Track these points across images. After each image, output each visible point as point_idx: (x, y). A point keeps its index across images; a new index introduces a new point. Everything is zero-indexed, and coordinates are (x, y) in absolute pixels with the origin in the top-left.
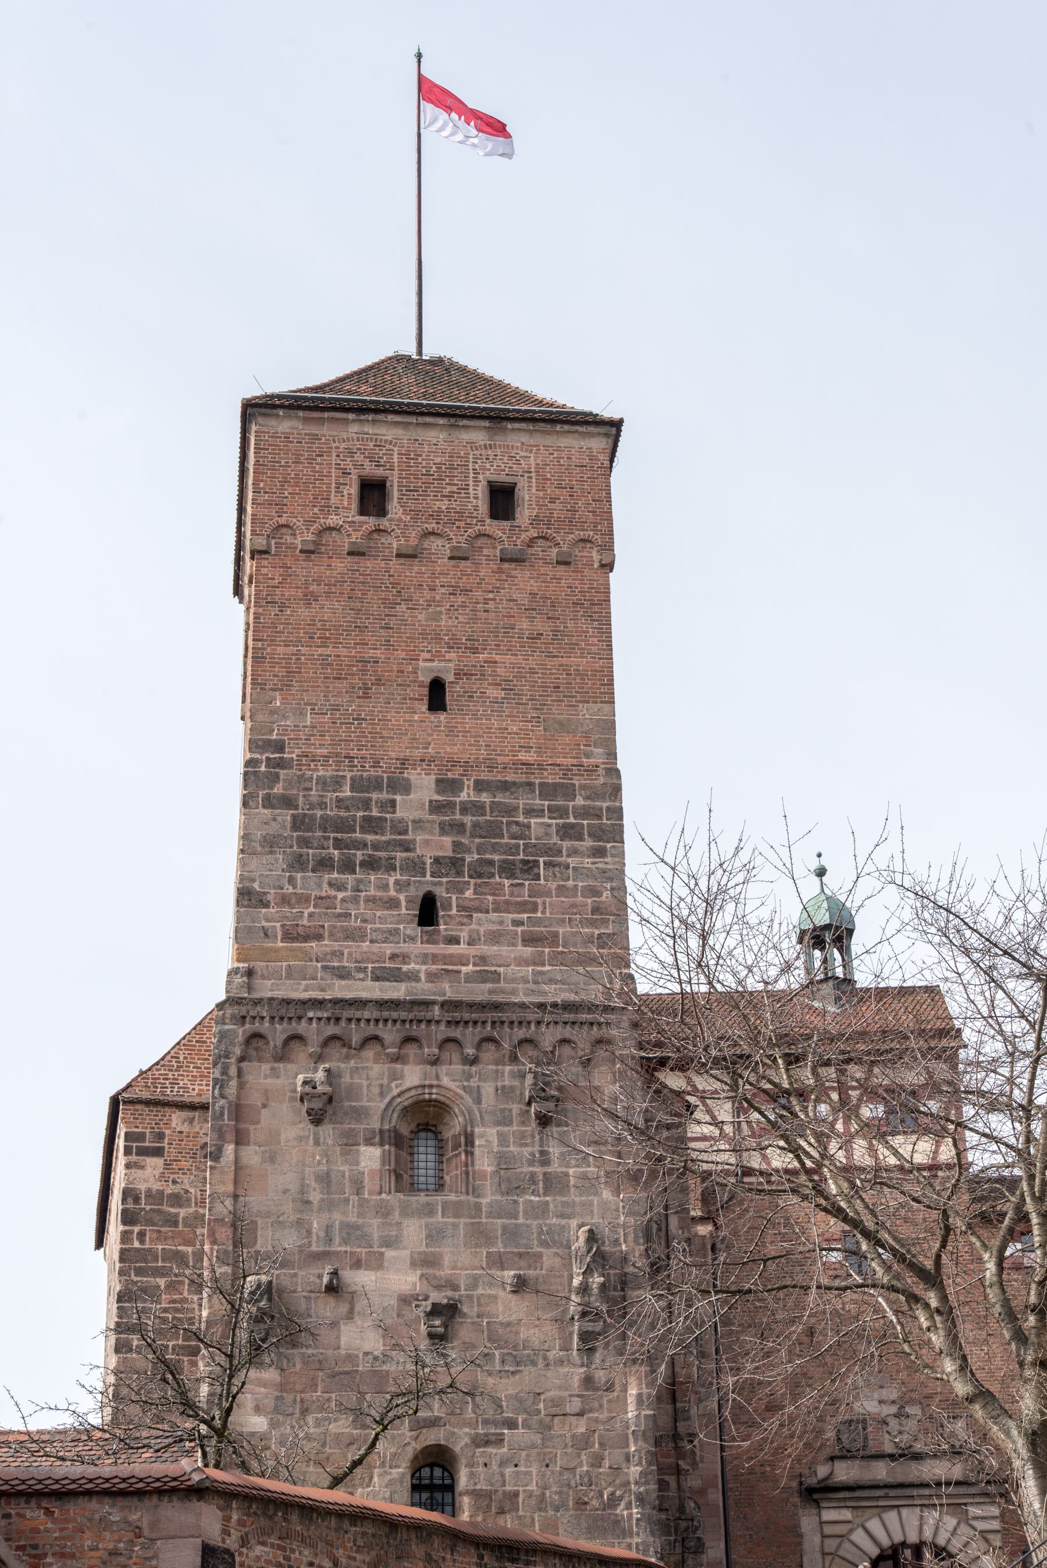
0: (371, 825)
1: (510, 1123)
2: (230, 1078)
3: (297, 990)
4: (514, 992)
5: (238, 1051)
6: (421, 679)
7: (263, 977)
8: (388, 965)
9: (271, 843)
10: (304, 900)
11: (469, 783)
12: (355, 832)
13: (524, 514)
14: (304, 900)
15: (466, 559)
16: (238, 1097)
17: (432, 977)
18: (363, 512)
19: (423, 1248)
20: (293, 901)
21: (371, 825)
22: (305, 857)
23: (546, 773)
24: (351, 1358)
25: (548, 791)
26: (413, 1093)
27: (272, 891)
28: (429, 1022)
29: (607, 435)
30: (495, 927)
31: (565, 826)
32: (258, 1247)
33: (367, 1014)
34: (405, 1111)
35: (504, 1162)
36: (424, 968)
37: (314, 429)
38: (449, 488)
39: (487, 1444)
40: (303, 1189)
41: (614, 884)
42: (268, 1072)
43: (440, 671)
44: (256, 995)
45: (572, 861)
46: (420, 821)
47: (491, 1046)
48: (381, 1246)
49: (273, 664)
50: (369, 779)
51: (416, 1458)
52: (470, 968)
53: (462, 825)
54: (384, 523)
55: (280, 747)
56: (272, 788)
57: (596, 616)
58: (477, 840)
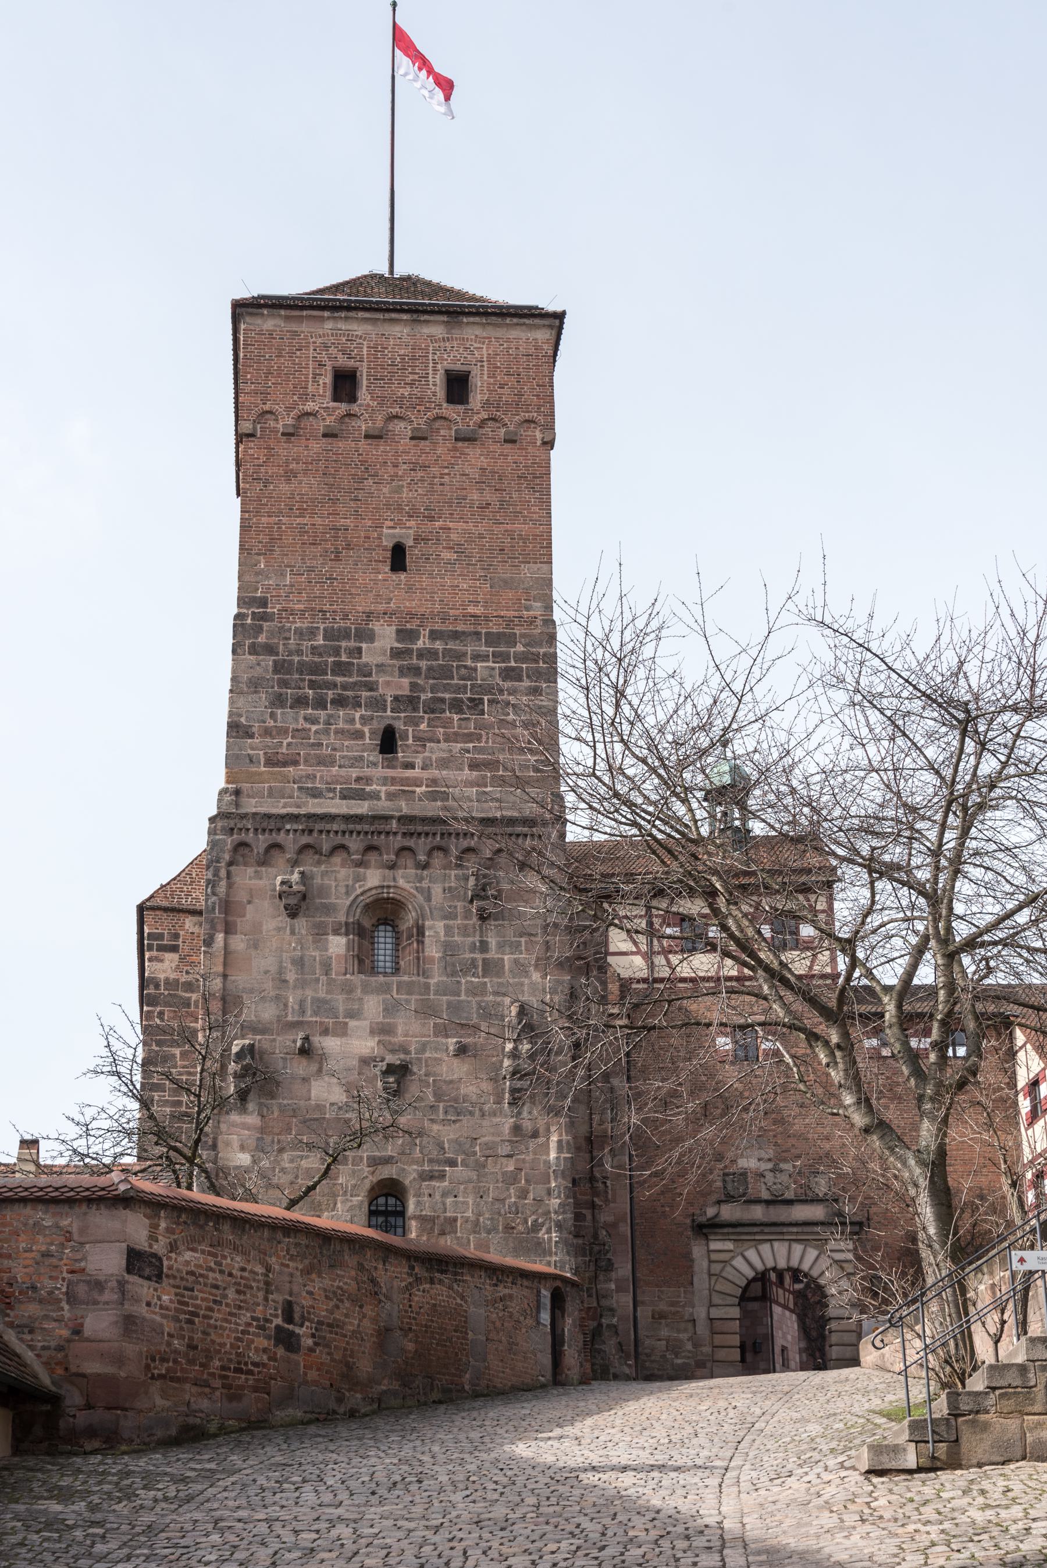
0: (341, 668)
1: (455, 918)
2: (220, 879)
3: (277, 807)
5: (227, 857)
6: (385, 543)
7: (249, 796)
8: (353, 786)
9: (255, 685)
10: (283, 732)
11: (425, 633)
12: (327, 674)
13: (477, 398)
14: (283, 732)
15: (425, 439)
16: (228, 895)
17: (391, 796)
18: (336, 398)
19: (381, 1019)
20: (274, 733)
21: (341, 668)
22: (284, 696)
23: (491, 624)
24: (320, 1108)
25: (492, 639)
26: (374, 892)
27: (257, 725)
28: (388, 833)
31: (507, 669)
33: (335, 827)
34: (367, 907)
35: (449, 949)
36: (384, 788)
38: (411, 377)
39: (432, 1178)
40: (281, 971)
42: (252, 875)
43: (401, 537)
46: (382, 665)
47: (441, 854)
48: (345, 1017)
49: (258, 532)
50: (339, 629)
51: (372, 1189)
52: (424, 788)
54: (355, 408)
55: (263, 603)
56: (257, 638)
57: (537, 488)
58: (431, 681)
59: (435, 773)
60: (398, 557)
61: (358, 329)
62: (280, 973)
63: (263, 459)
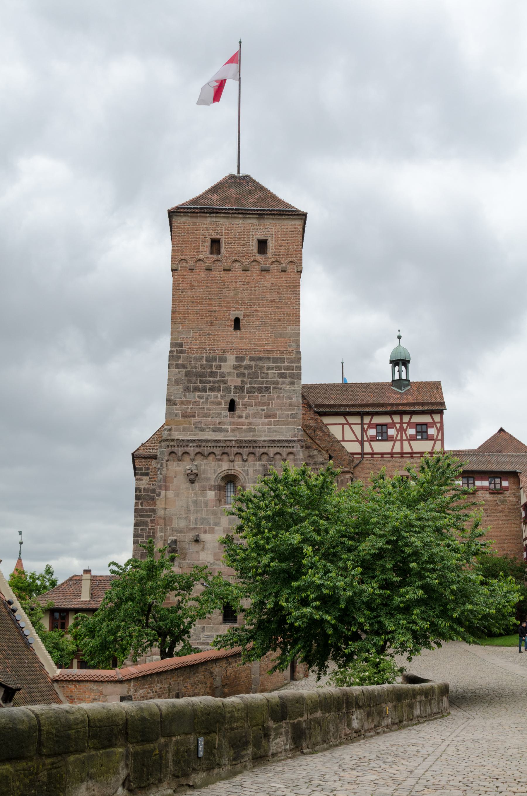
3: (186, 436)
4: (261, 436)
5: (166, 458)
6: (231, 318)
7: (175, 431)
10: (189, 402)
14: (189, 402)
15: (249, 270)
17: (233, 430)
18: (212, 253)
19: (228, 526)
25: (275, 360)
26: (225, 472)
28: (231, 447)
29: (301, 219)
30: (256, 412)
32: (173, 526)
33: (210, 444)
36: (229, 427)
37: (194, 220)
41: (297, 395)
44: (173, 438)
45: (283, 387)
46: (230, 372)
47: (252, 455)
48: (213, 525)
52: (246, 427)
53: (244, 374)
54: (219, 257)
55: (181, 345)
58: (249, 379)
59: (250, 420)
61: (221, 221)
62: (187, 507)
63: (181, 280)
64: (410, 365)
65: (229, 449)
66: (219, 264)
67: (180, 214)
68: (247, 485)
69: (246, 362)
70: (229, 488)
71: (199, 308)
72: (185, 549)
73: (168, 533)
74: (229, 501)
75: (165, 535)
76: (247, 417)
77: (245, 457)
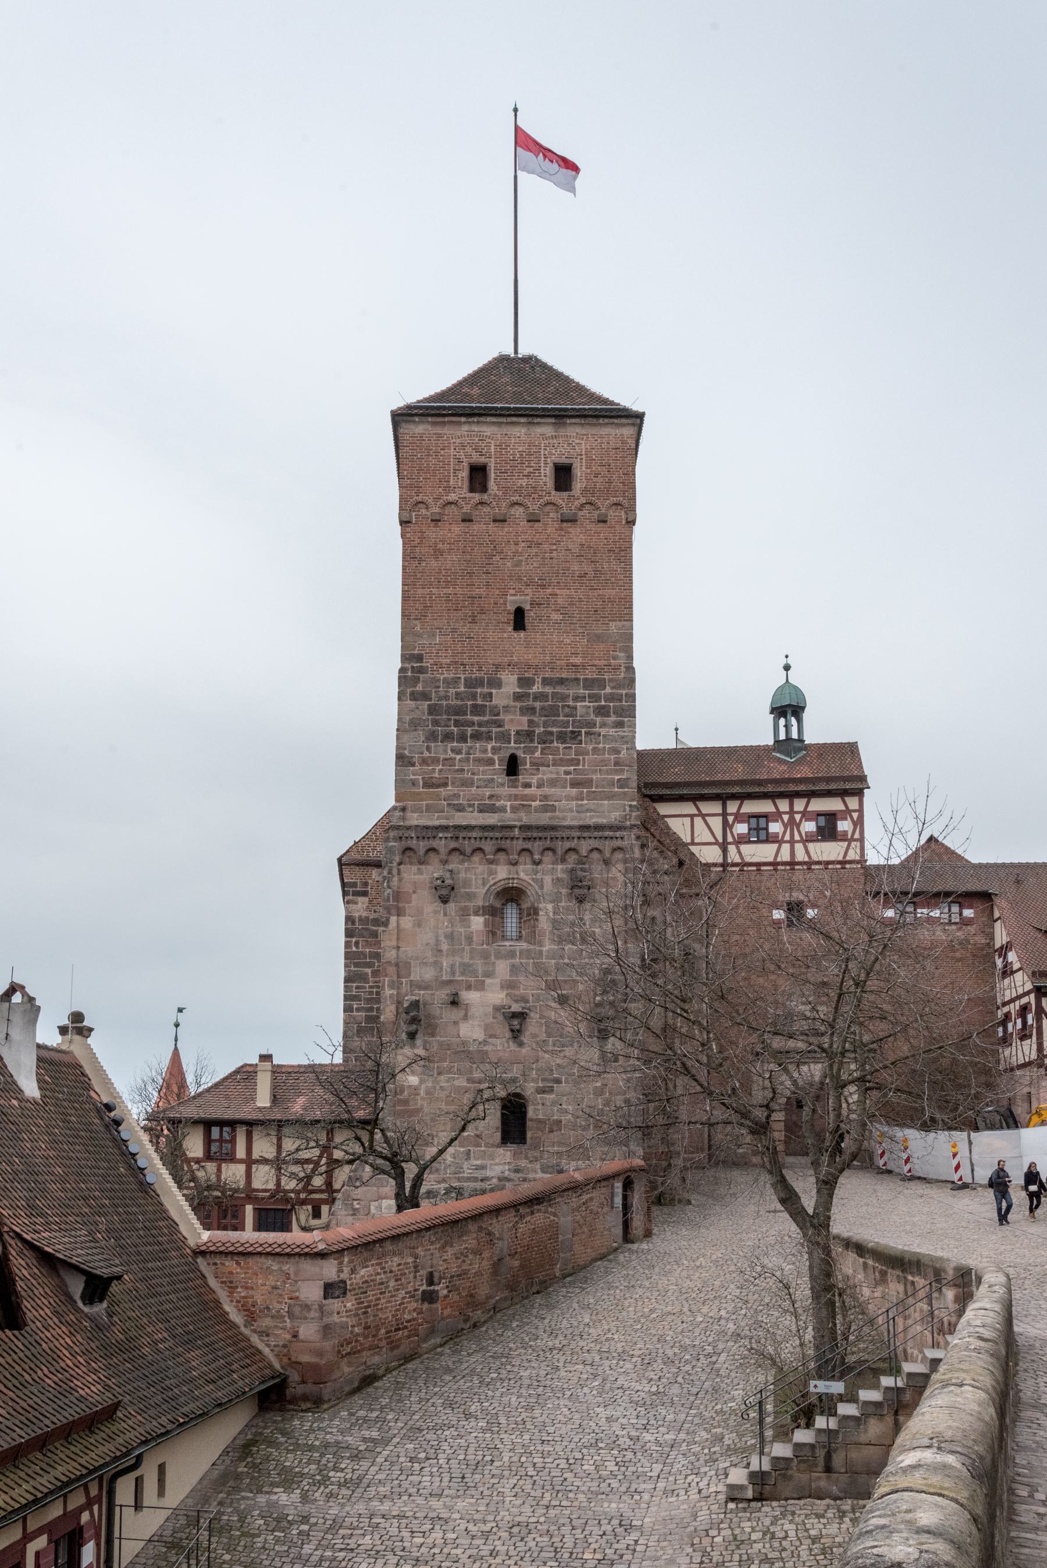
0: (477, 710)
2: (393, 876)
5: (397, 859)
7: (413, 812)
10: (436, 761)
13: (578, 486)
14: (436, 761)
15: (539, 521)
17: (514, 810)
18: (472, 490)
19: (508, 978)
21: (477, 710)
25: (589, 684)
28: (512, 838)
29: (633, 425)
32: (412, 978)
33: (474, 834)
34: (498, 894)
35: (555, 924)
36: (509, 803)
37: (439, 430)
39: (544, 1092)
40: (438, 942)
44: (408, 823)
45: (603, 731)
46: (507, 706)
47: (550, 853)
50: (476, 679)
52: (538, 803)
53: (534, 709)
54: (485, 497)
55: (419, 658)
59: (546, 790)
60: (519, 619)
61: (488, 430)
63: (417, 541)
64: (806, 715)
65: (508, 841)
66: (486, 509)
67: (413, 418)
68: (541, 906)
69: (536, 688)
70: (509, 911)
71: (450, 591)
72: (434, 1018)
73: (404, 991)
74: (509, 934)
75: (398, 994)
76: (539, 786)
77: (537, 857)
